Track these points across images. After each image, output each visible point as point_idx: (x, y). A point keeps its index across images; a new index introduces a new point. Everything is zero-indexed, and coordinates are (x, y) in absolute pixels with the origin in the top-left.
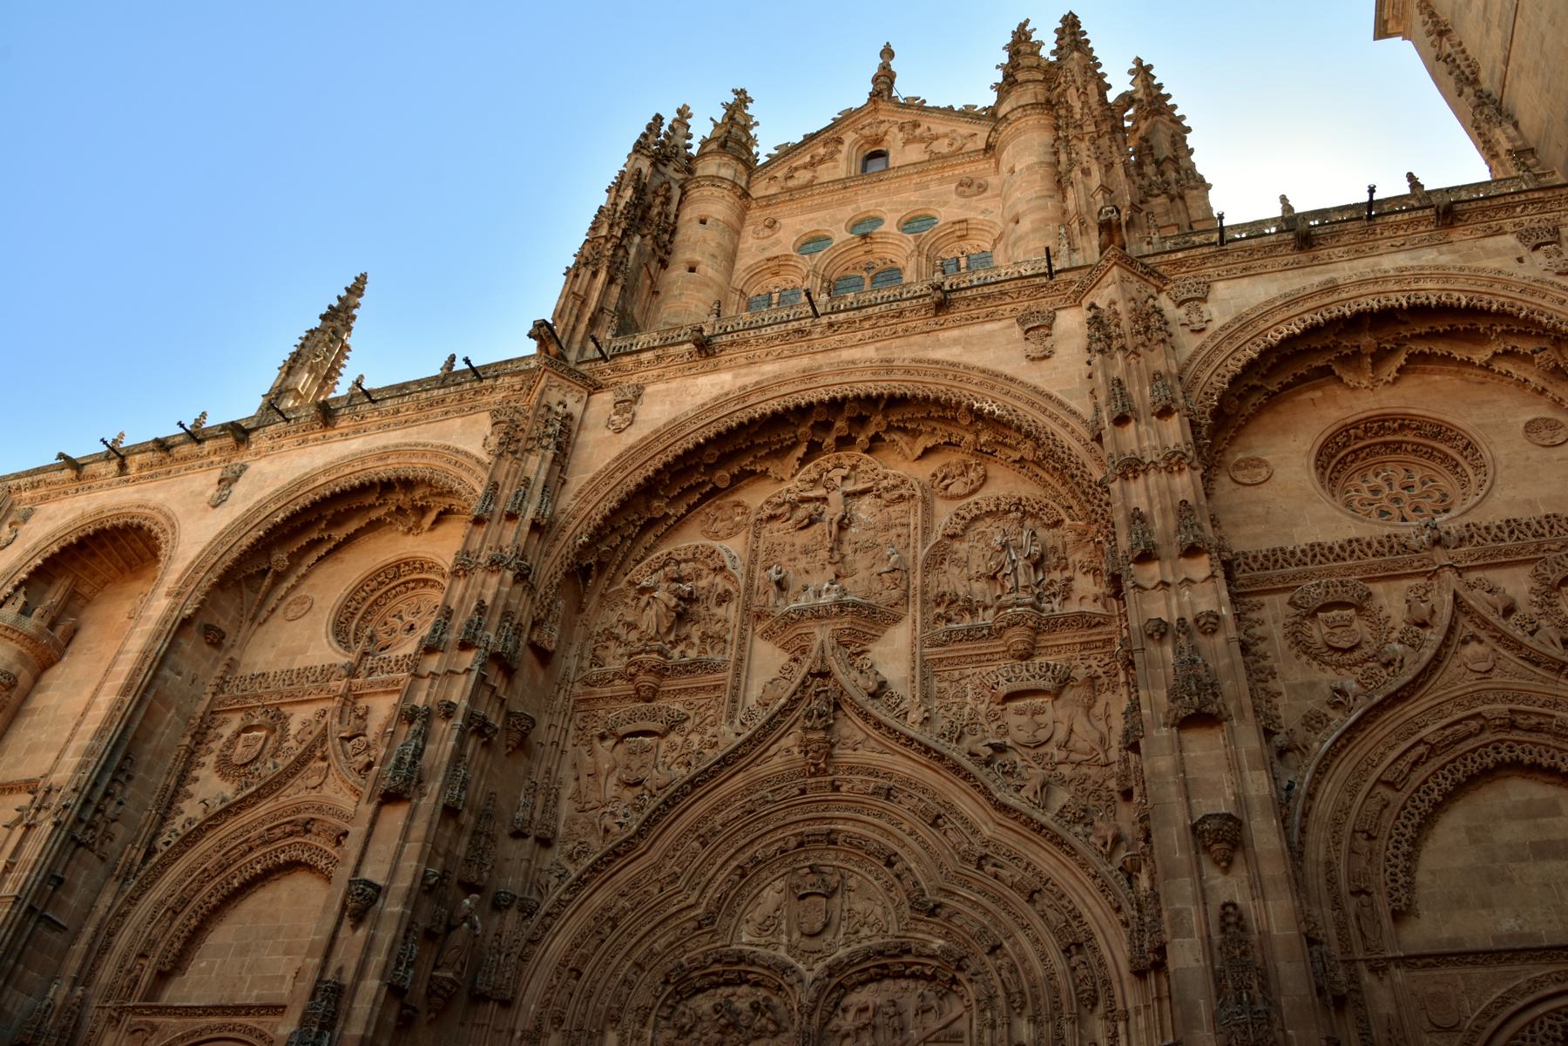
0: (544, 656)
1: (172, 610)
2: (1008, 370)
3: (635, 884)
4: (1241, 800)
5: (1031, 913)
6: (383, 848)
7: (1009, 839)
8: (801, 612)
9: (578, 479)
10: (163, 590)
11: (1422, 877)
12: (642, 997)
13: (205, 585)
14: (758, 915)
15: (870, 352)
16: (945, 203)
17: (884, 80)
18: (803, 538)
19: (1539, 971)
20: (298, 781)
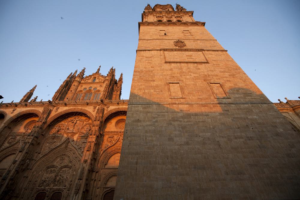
0: (43, 135)
1: (4, 125)
2: (91, 112)
3: (46, 158)
4: (88, 158)
5: (78, 162)
6: (18, 157)
7: (79, 156)
8: (68, 132)
9: (50, 117)
10: (3, 123)
11: (109, 161)
12: (44, 169)
13: (9, 123)
14: (56, 161)
15: (80, 107)
16: (98, 87)
17: (99, 70)
18: (72, 124)
19: (112, 170)
20: (16, 145)
